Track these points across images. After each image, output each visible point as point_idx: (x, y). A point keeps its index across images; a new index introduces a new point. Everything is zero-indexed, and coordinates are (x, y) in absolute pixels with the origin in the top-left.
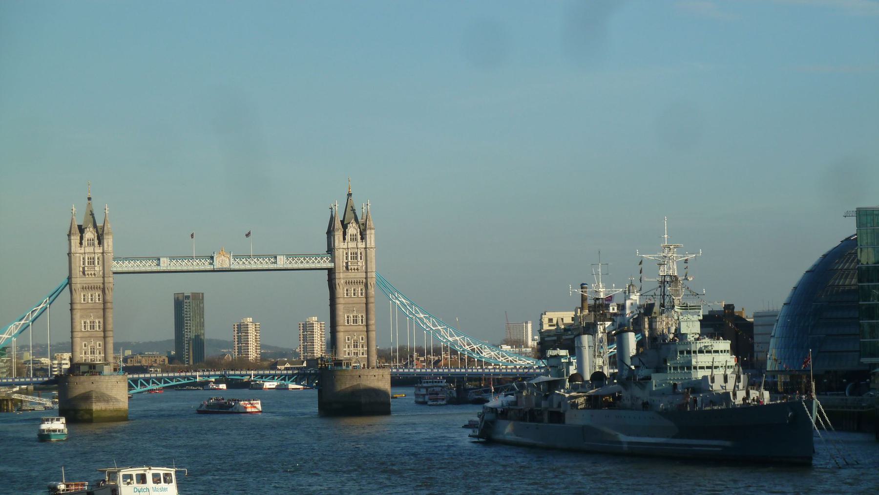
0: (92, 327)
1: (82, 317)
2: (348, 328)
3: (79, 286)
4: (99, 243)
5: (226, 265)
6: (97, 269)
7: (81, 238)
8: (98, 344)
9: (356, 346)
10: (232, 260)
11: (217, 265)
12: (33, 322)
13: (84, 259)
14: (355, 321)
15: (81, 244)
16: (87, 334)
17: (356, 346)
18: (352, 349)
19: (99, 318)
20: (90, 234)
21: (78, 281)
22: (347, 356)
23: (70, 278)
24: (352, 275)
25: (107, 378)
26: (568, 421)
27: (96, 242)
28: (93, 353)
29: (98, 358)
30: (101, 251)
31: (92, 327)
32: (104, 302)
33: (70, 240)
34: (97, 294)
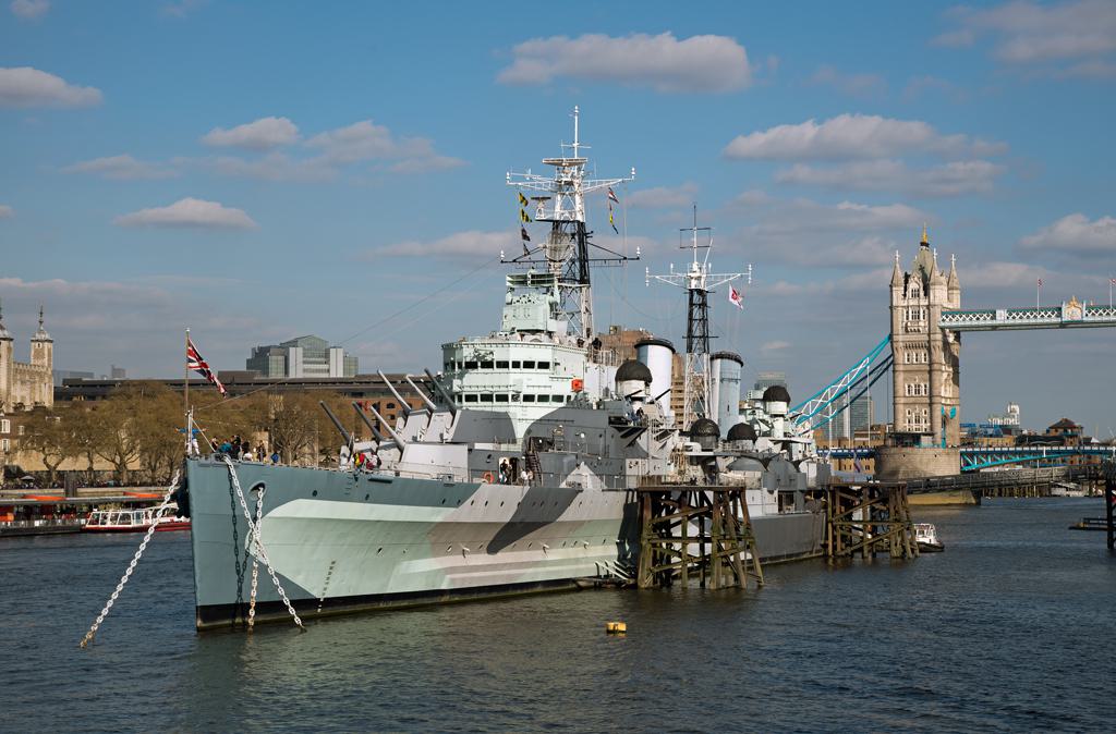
1: (905, 379)
4: (925, 295)
5: (1078, 317)
6: (922, 324)
8: (923, 411)
10: (1085, 312)
11: (1066, 317)
12: (870, 385)
13: (907, 312)
15: (905, 295)
16: (912, 400)
19: (925, 381)
21: (900, 338)
23: (891, 337)
27: (922, 293)
28: (918, 421)
29: (924, 426)
30: (927, 303)
32: (931, 364)
33: (892, 291)
34: (922, 353)
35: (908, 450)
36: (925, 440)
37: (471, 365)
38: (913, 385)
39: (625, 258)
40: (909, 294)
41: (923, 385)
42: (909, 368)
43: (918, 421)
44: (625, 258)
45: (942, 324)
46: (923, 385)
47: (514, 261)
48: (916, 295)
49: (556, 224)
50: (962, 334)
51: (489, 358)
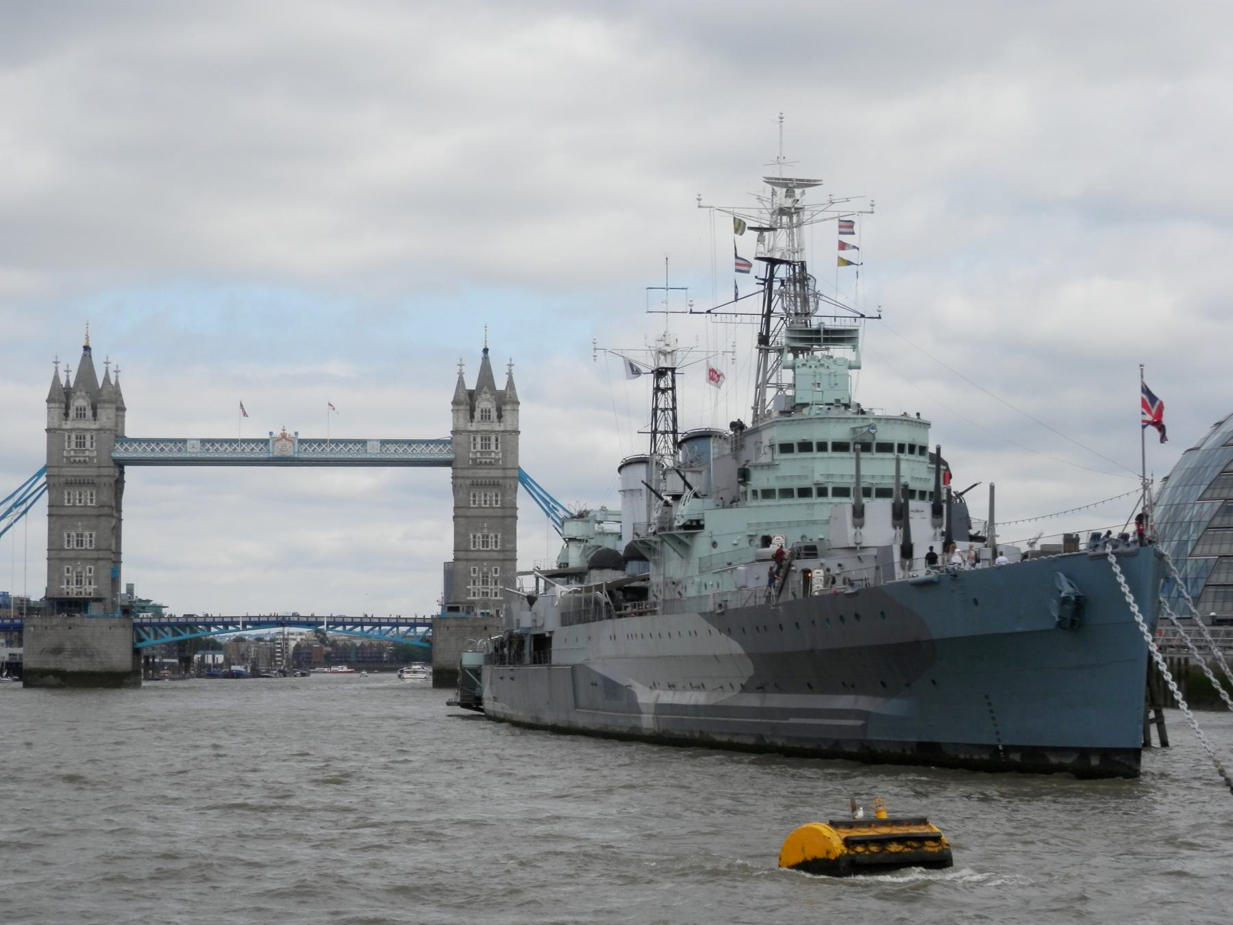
0: (80, 543)
2: (474, 555)
3: (63, 480)
4: (95, 415)
6: (87, 453)
7: (67, 408)
9: (485, 582)
13: (69, 437)
14: (485, 543)
15: (66, 415)
16: (72, 555)
17: (485, 582)
18: (479, 586)
20: (80, 402)
22: (471, 598)
24: (482, 473)
25: (93, 621)
26: (556, 658)
27: (89, 413)
28: (79, 582)
29: (89, 589)
31: (80, 543)
35: (78, 618)
36: (94, 609)
37: (840, 447)
38: (73, 534)
39: (862, 316)
40: (72, 413)
41: (87, 533)
42: (71, 511)
43: (79, 582)
44: (862, 316)
45: (116, 455)
46: (87, 533)
47: (709, 312)
48: (81, 414)
49: (773, 262)
50: (128, 469)
51: (868, 439)
